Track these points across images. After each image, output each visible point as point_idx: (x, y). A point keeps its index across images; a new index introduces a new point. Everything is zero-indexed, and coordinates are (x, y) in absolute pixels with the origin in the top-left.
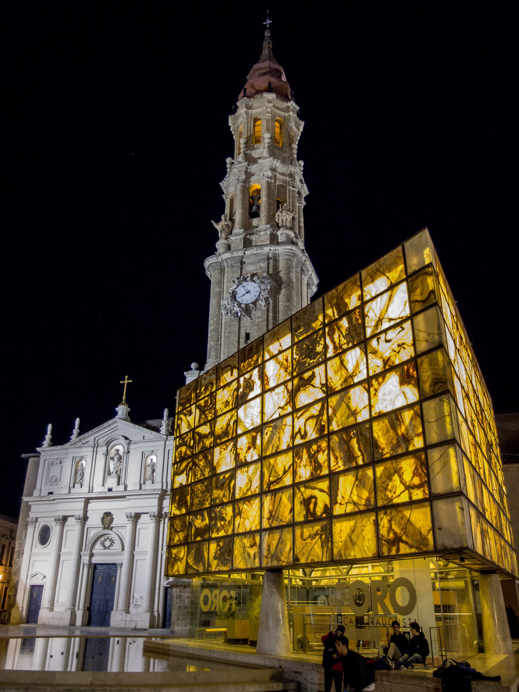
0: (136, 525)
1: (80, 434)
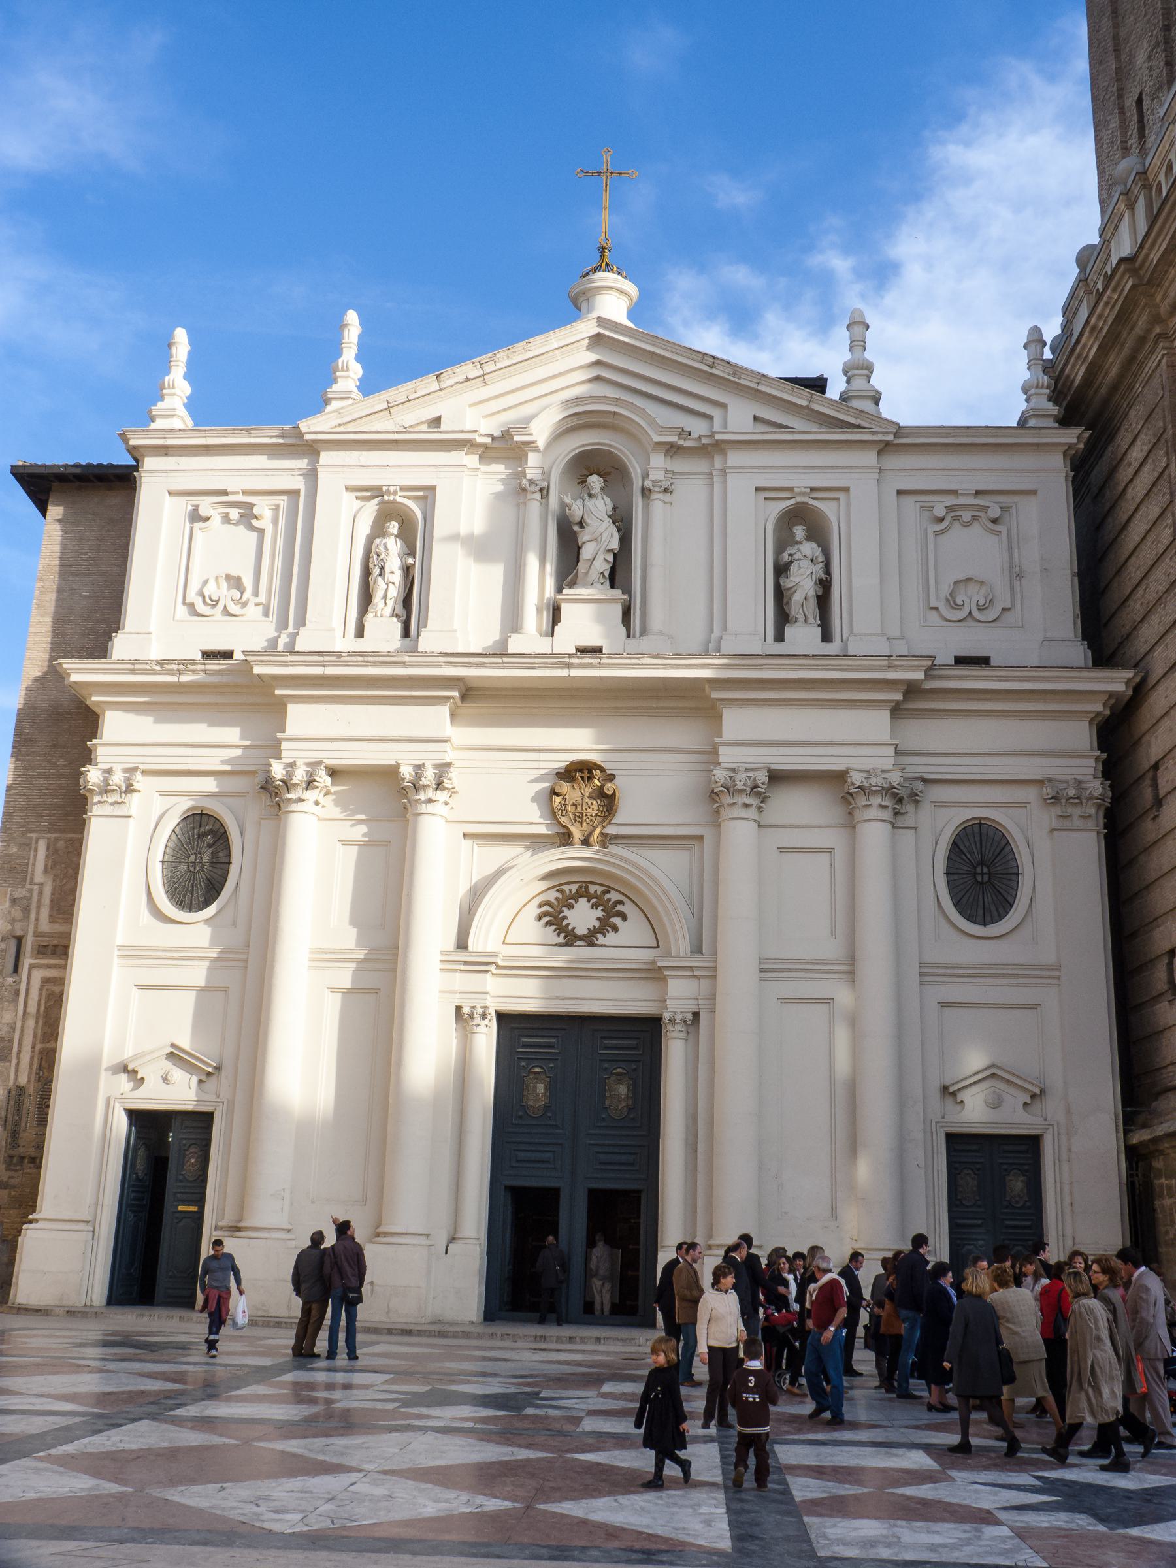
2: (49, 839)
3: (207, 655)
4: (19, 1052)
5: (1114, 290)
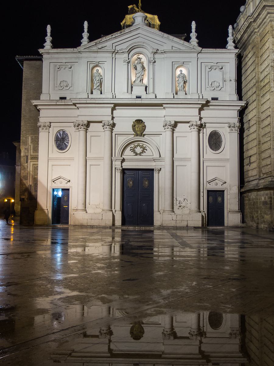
0: (173, 133)
1: (91, 39)
2: (31, 136)
3: (62, 98)
4: (29, 178)
5: (247, 22)
